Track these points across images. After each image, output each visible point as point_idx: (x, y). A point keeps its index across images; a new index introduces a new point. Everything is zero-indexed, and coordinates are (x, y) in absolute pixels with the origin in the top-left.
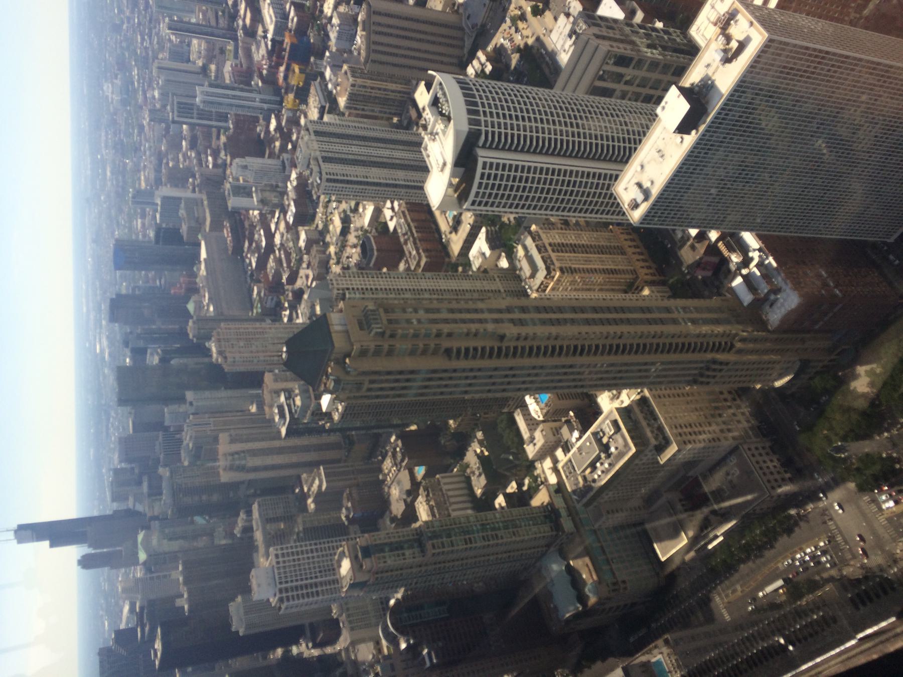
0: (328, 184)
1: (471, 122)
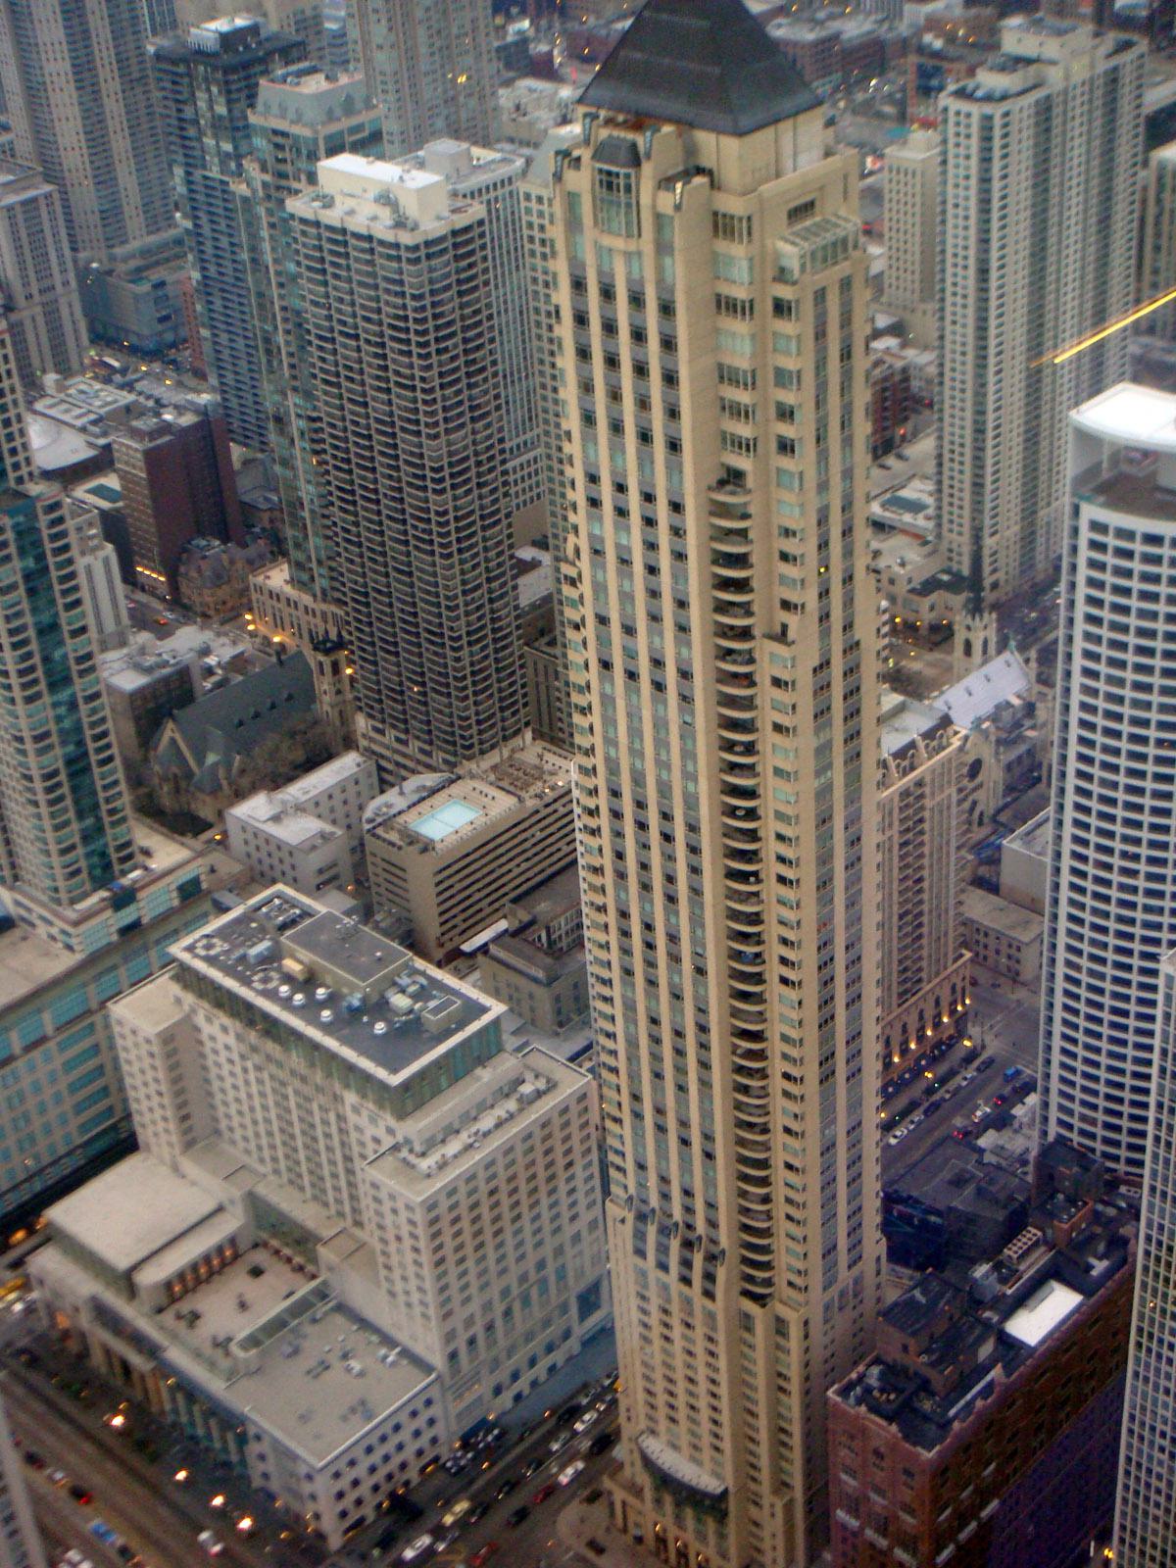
0: (975, 121)
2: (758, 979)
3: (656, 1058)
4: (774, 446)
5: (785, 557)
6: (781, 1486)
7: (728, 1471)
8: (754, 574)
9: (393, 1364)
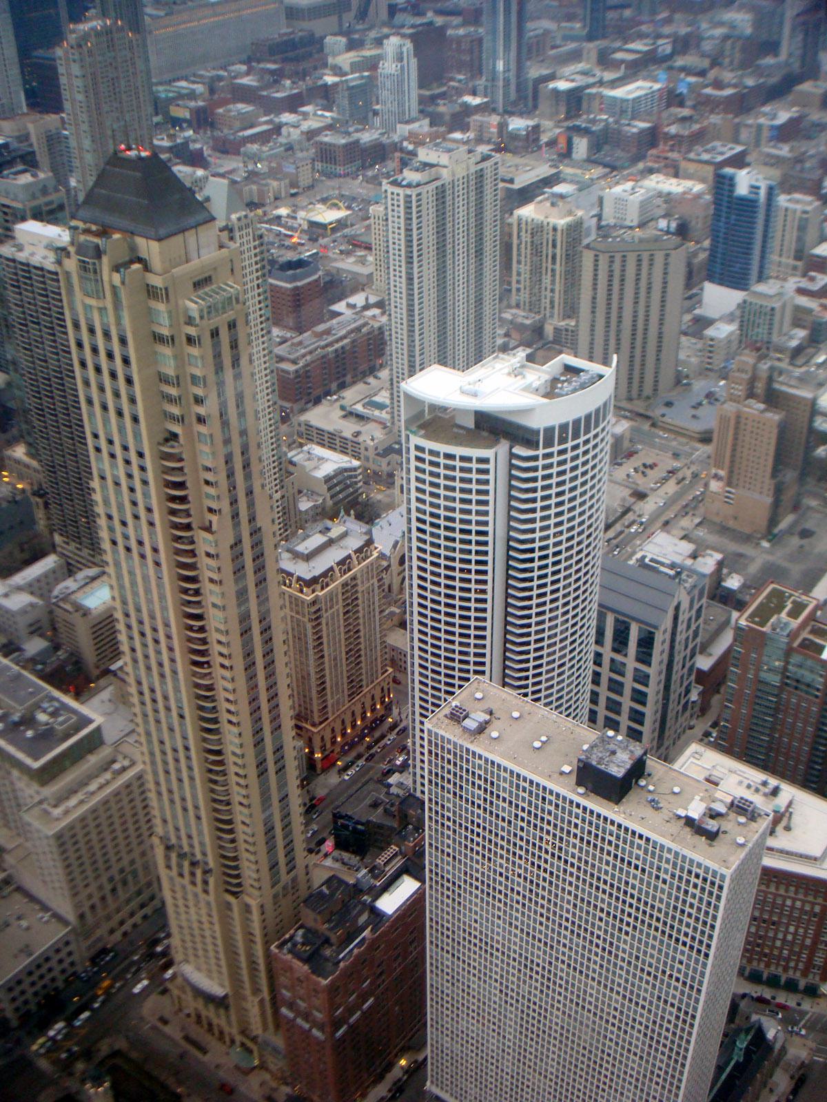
0: (402, 198)
1: (549, 431)
2: (215, 721)
3: (165, 763)
4: (194, 419)
5: (207, 483)
6: (256, 990)
7: (227, 983)
8: (190, 492)
9: (47, 922)
